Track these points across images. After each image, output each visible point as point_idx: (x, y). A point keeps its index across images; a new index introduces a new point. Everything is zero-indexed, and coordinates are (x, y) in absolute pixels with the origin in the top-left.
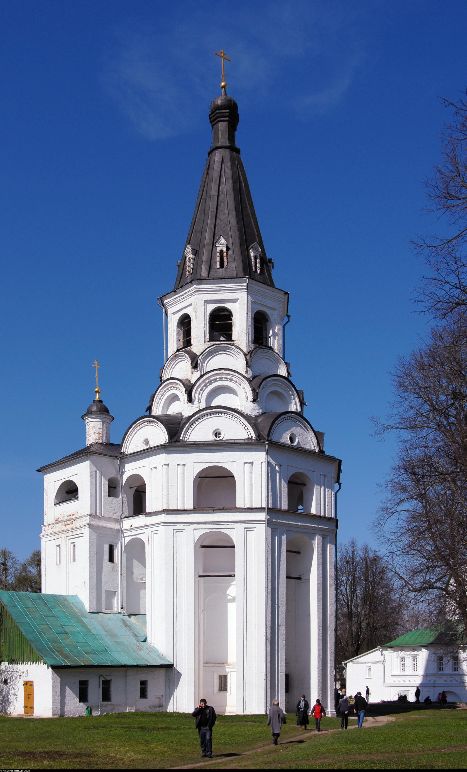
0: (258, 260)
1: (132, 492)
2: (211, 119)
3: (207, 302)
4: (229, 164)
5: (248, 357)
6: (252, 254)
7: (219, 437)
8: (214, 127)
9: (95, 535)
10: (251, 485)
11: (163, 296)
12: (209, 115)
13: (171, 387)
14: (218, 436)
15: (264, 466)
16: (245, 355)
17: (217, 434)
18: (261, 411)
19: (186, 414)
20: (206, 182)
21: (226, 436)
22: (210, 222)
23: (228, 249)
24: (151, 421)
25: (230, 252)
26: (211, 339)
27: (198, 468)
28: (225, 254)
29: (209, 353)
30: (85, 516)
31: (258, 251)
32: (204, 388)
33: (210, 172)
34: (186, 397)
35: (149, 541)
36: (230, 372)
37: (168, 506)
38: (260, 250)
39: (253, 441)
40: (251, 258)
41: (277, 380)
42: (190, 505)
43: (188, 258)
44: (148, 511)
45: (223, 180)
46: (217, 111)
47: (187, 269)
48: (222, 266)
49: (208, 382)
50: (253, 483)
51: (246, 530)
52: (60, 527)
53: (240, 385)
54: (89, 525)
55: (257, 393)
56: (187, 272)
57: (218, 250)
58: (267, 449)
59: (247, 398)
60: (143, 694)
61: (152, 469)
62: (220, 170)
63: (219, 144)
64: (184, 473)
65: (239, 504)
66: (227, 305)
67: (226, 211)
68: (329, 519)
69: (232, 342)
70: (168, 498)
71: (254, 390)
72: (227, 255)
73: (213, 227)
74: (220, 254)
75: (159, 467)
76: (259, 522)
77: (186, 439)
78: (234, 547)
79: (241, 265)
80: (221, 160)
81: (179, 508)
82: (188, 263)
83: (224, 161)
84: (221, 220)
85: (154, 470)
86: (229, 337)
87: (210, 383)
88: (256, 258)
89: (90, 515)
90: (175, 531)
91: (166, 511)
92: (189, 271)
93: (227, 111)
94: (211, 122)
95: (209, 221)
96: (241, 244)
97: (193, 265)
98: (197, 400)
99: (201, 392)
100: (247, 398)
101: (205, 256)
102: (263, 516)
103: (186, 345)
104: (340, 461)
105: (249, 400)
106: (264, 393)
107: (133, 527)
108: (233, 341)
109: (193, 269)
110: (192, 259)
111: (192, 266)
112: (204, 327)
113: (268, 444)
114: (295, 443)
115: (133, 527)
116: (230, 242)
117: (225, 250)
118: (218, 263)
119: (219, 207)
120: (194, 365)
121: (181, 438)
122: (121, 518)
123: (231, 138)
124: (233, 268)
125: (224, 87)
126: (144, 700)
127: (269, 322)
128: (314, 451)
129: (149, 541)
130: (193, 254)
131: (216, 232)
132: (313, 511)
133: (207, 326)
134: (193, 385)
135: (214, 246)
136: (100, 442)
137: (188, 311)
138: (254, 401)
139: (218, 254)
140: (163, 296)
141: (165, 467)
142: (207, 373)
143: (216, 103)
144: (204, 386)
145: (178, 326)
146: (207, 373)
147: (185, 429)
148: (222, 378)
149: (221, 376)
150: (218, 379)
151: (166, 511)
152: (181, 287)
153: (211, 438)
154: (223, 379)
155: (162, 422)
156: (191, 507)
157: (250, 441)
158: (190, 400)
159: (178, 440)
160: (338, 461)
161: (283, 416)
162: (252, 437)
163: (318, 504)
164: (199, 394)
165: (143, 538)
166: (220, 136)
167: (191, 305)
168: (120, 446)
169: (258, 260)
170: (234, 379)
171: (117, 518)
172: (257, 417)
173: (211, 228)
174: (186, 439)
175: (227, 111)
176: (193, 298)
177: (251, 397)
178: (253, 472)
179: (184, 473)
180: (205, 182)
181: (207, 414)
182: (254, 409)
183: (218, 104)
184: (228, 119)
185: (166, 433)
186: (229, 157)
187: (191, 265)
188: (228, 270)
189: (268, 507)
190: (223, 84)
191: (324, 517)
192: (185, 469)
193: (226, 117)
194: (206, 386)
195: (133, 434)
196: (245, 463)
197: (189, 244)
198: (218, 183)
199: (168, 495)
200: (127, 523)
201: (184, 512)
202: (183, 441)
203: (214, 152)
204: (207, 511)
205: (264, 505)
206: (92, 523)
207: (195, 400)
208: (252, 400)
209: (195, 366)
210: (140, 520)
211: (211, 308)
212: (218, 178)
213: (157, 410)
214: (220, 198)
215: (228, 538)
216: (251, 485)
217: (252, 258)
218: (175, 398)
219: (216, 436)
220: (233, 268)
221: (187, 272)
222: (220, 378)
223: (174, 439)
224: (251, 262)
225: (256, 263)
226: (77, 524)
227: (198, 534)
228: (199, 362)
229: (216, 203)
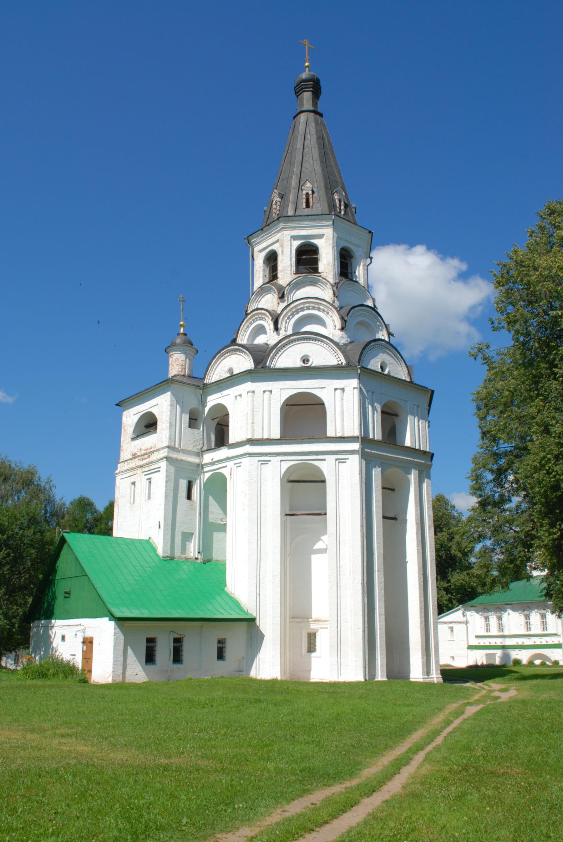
0: (342, 203)
1: (214, 424)
2: (297, 91)
3: (294, 238)
4: (313, 124)
5: (335, 289)
6: (336, 197)
7: (307, 364)
8: (299, 97)
9: (173, 469)
10: (343, 412)
11: (250, 236)
12: (295, 88)
13: (256, 318)
14: (306, 362)
15: (356, 392)
16: (332, 286)
17: (305, 360)
18: (349, 340)
19: (272, 342)
20: (292, 139)
21: (315, 362)
22: (296, 170)
24: (236, 350)
25: (316, 195)
26: (297, 272)
27: (286, 395)
28: (311, 196)
29: (296, 285)
30: (163, 448)
31: (342, 195)
32: (291, 317)
33: (295, 130)
34: (272, 326)
35: (231, 475)
36: (318, 301)
37: (253, 435)
38: (344, 194)
40: (335, 201)
41: (365, 311)
42: (276, 434)
43: (274, 202)
44: (230, 442)
45: (308, 136)
46: (302, 83)
47: (274, 211)
48: (308, 206)
49: (295, 311)
50: (345, 410)
51: (337, 462)
52: (137, 462)
53: (328, 313)
54: (167, 458)
55: (346, 321)
56: (274, 214)
57: (304, 192)
58: (360, 374)
59: (335, 326)
60: (221, 655)
61: (236, 397)
62: (305, 128)
63: (304, 109)
64: (270, 400)
65: (330, 433)
66: (315, 241)
67: (311, 161)
68: (425, 452)
69: (319, 275)
70: (253, 427)
71: (342, 318)
72: (313, 197)
73: (299, 173)
74: (306, 196)
75: (244, 394)
76: (352, 452)
77: (272, 365)
78: (324, 481)
79: (326, 205)
80: (306, 121)
81: (265, 437)
82: (274, 206)
83: (309, 121)
84: (306, 169)
85: (238, 398)
86: (316, 270)
87: (297, 312)
88: (340, 201)
89: (168, 447)
90: (260, 463)
91: (251, 442)
92: (275, 213)
93: (311, 83)
94: (296, 93)
95: (295, 169)
96: (326, 188)
97: (280, 207)
98: (283, 329)
99: (288, 321)
100: (335, 326)
101: (292, 198)
102: (356, 446)
103: (271, 279)
104: (433, 392)
105: (337, 329)
106: (352, 322)
108: (320, 273)
109: (279, 210)
110: (279, 202)
111: (278, 208)
112: (291, 261)
113: (360, 368)
114: (386, 372)
116: (316, 186)
117: (310, 192)
118: (304, 204)
119: (304, 158)
120: (280, 295)
121: (267, 365)
122: (202, 452)
123: (315, 104)
124: (318, 208)
126: (221, 662)
127: (353, 259)
128: (405, 381)
129: (231, 475)
130: (279, 198)
131: (302, 178)
132: (408, 443)
133: (294, 259)
134: (279, 315)
135: (300, 189)
136: (183, 374)
137: (275, 247)
138: (342, 329)
139: (304, 196)
140: (250, 236)
141: (250, 394)
142: (293, 302)
143: (301, 77)
144: (291, 315)
145: (264, 263)
146: (293, 302)
147: (271, 355)
148: (309, 306)
149: (308, 305)
150: (305, 308)
151: (251, 442)
152: (268, 225)
153: (299, 364)
154: (311, 308)
156: (278, 437)
158: (276, 329)
159: (264, 367)
160: (430, 391)
161: (373, 344)
162: (342, 363)
163: (413, 435)
164: (286, 322)
166: (305, 103)
167: (277, 241)
168: (204, 378)
169: (342, 203)
170: (322, 307)
171: (196, 451)
172: (345, 345)
173: (297, 175)
174: (272, 365)
175: (311, 83)
176: (280, 234)
178: (344, 398)
179: (270, 400)
180: (291, 139)
181: (295, 340)
182: (342, 338)
183: (302, 78)
184: (311, 89)
185: (252, 360)
186: (313, 118)
187: (278, 207)
188: (314, 209)
189: (361, 436)
190: (307, 64)
191: (419, 450)
192: (272, 396)
193: (310, 88)
194: (293, 315)
195: (216, 365)
196: (336, 389)
197: (276, 189)
198: (303, 138)
199: (253, 423)
200: (208, 458)
201: (270, 442)
202: (269, 367)
203: (299, 116)
204: (295, 441)
205: (357, 433)
206: (171, 455)
207: (281, 329)
208: (341, 328)
209: (282, 297)
210: (223, 453)
211: (297, 243)
212: (304, 135)
213: (243, 339)
214: (305, 150)
216: (343, 412)
217: (337, 201)
218: (261, 330)
219: (304, 362)
220: (318, 208)
221: (274, 214)
222: (307, 307)
223: (261, 366)
224: (336, 204)
225: (340, 205)
227: (286, 466)
228: (285, 293)
229: (302, 154)
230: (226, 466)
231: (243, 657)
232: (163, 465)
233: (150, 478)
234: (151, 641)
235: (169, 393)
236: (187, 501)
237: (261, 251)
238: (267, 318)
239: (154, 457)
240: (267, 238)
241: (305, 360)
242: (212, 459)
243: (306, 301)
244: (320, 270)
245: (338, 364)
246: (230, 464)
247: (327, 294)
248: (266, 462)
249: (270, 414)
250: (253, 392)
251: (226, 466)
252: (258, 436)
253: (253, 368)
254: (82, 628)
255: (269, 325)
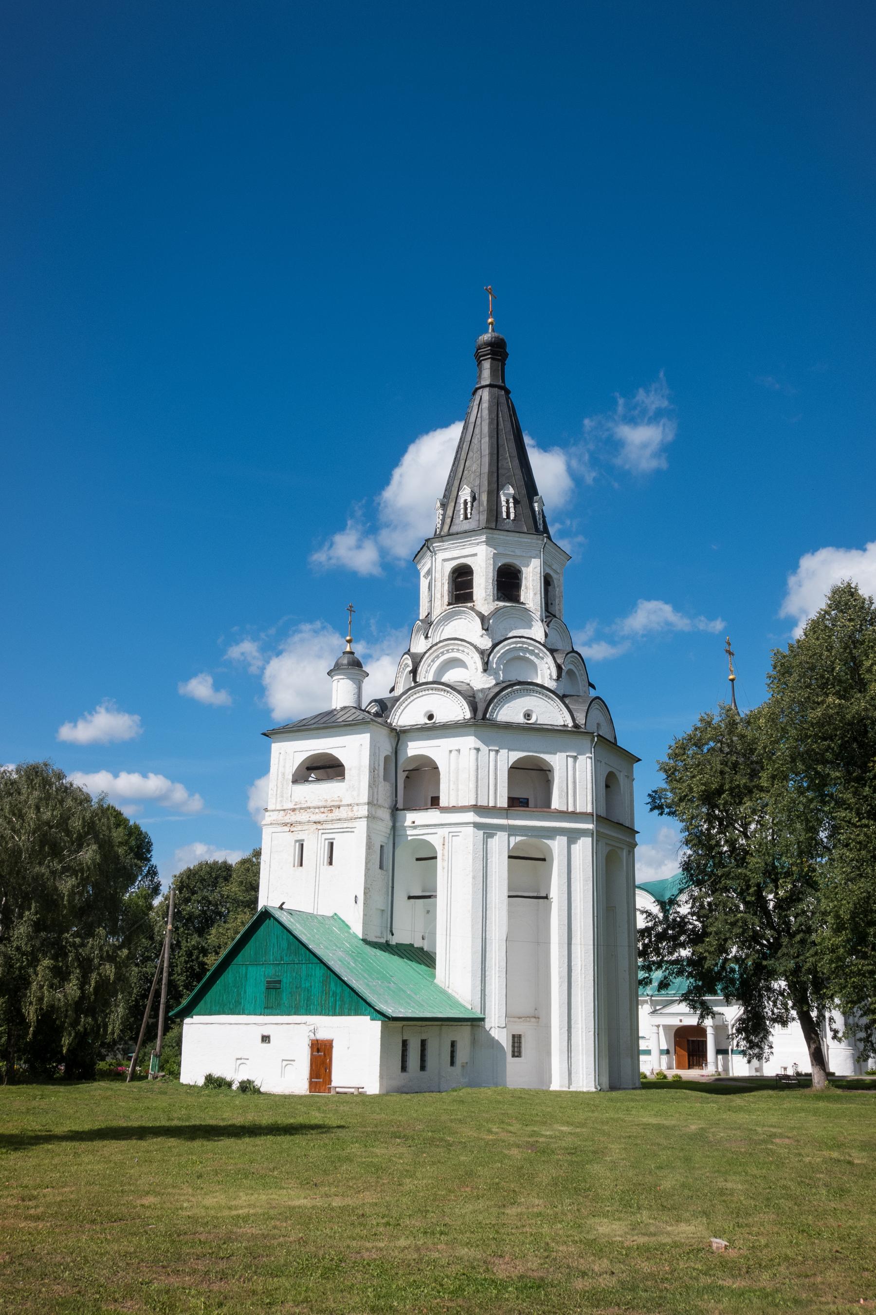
10: (574, 782)
17: (528, 716)
23: (514, 498)
39: (569, 729)
42: (503, 802)
61: (451, 751)
64: (496, 761)
66: (516, 562)
85: (454, 753)
107: (416, 824)
115: (416, 824)
121: (487, 716)
125: (492, 323)
153: (520, 719)
155: (459, 692)
157: (565, 729)
165: (435, 840)
167: (475, 555)
177: (555, 676)
179: (496, 761)
190: (490, 320)
215: (550, 850)
216: (574, 782)
226: (343, 813)
227: (514, 840)
230: (436, 833)
231: (467, 1063)
232: (362, 827)
233: (334, 839)
234: (405, 1043)
235: (367, 736)
236: (380, 871)
237: (445, 560)
238: (466, 650)
239: (343, 813)
240: (458, 546)
241: (528, 716)
242: (414, 822)
243: (518, 639)
244: (522, 599)
245: (564, 725)
246: (445, 831)
247: (538, 631)
248: (491, 836)
249: (496, 779)
250: (478, 750)
251: (436, 833)
252: (482, 802)
253: (468, 715)
254: (312, 1028)
255: (475, 661)
